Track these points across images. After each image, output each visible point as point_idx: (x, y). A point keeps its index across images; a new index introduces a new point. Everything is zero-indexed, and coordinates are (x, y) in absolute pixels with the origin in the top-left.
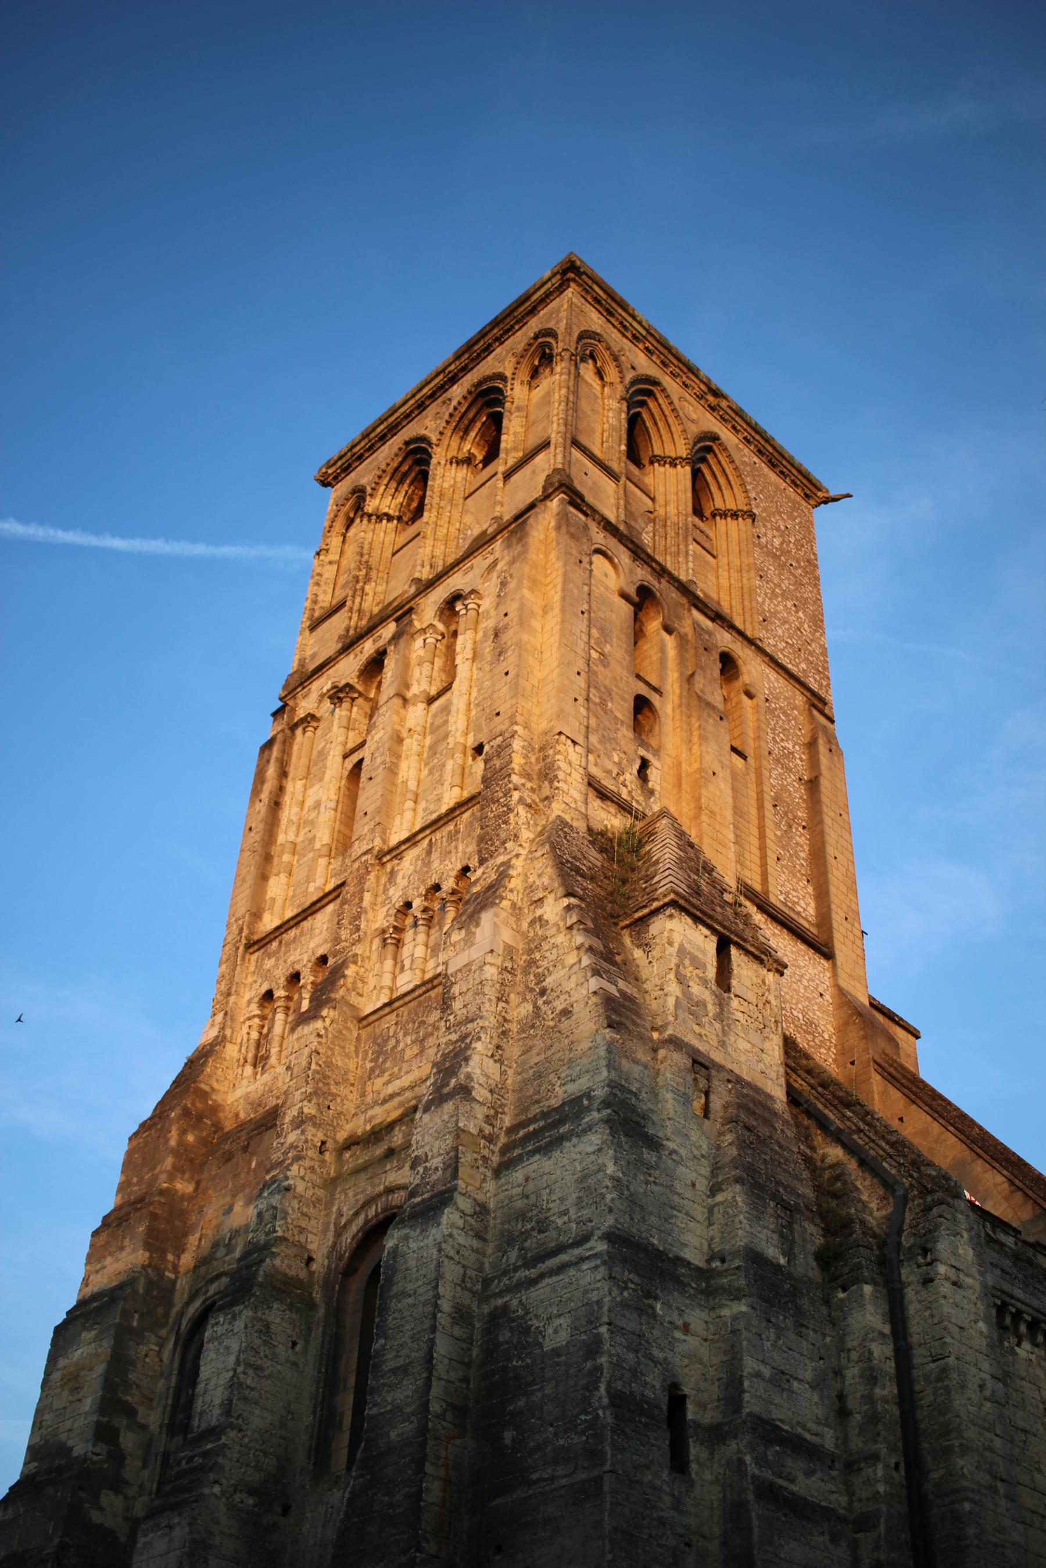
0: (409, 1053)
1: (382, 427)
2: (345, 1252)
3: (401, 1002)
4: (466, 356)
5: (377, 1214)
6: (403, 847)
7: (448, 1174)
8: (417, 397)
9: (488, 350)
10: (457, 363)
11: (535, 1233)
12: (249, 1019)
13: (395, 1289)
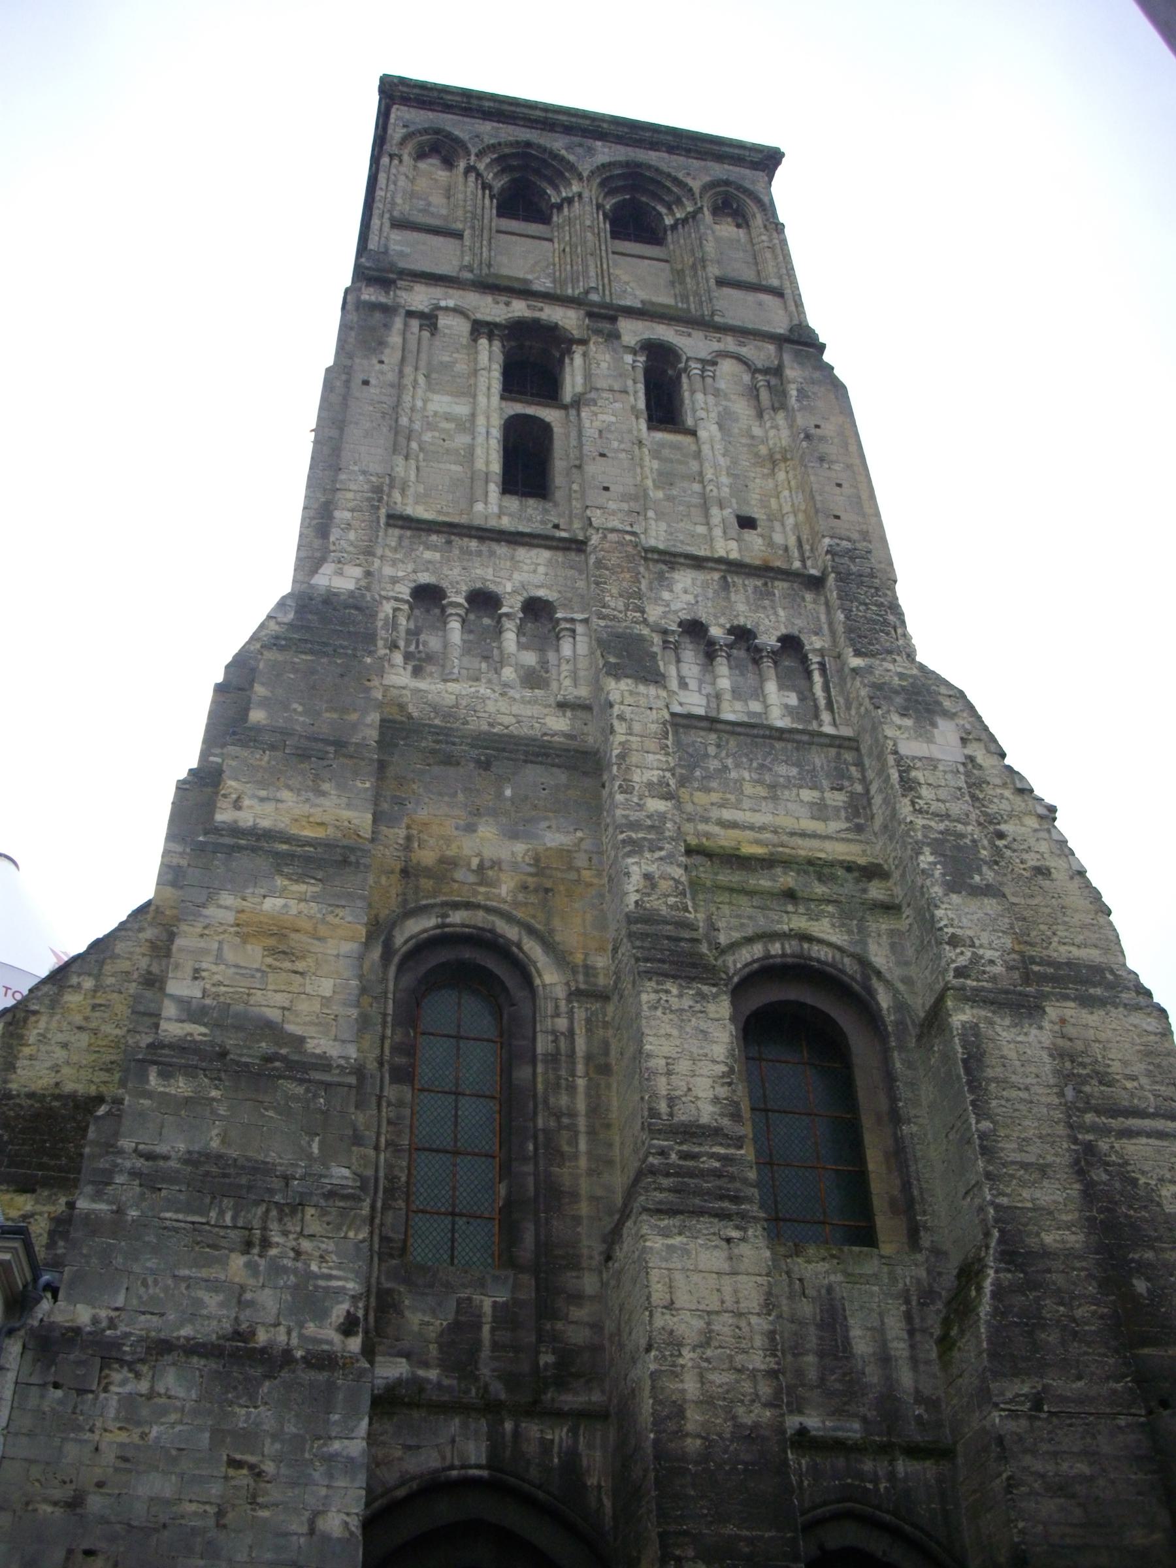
0: (748, 789)
1: (491, 104)
2: (734, 974)
3: (728, 728)
4: (626, 130)
5: (784, 955)
6: (682, 560)
7: (1016, 975)
8: (550, 115)
9: (688, 152)
10: (612, 127)
11: (1095, 1082)
12: (396, 599)
13: (990, 1073)
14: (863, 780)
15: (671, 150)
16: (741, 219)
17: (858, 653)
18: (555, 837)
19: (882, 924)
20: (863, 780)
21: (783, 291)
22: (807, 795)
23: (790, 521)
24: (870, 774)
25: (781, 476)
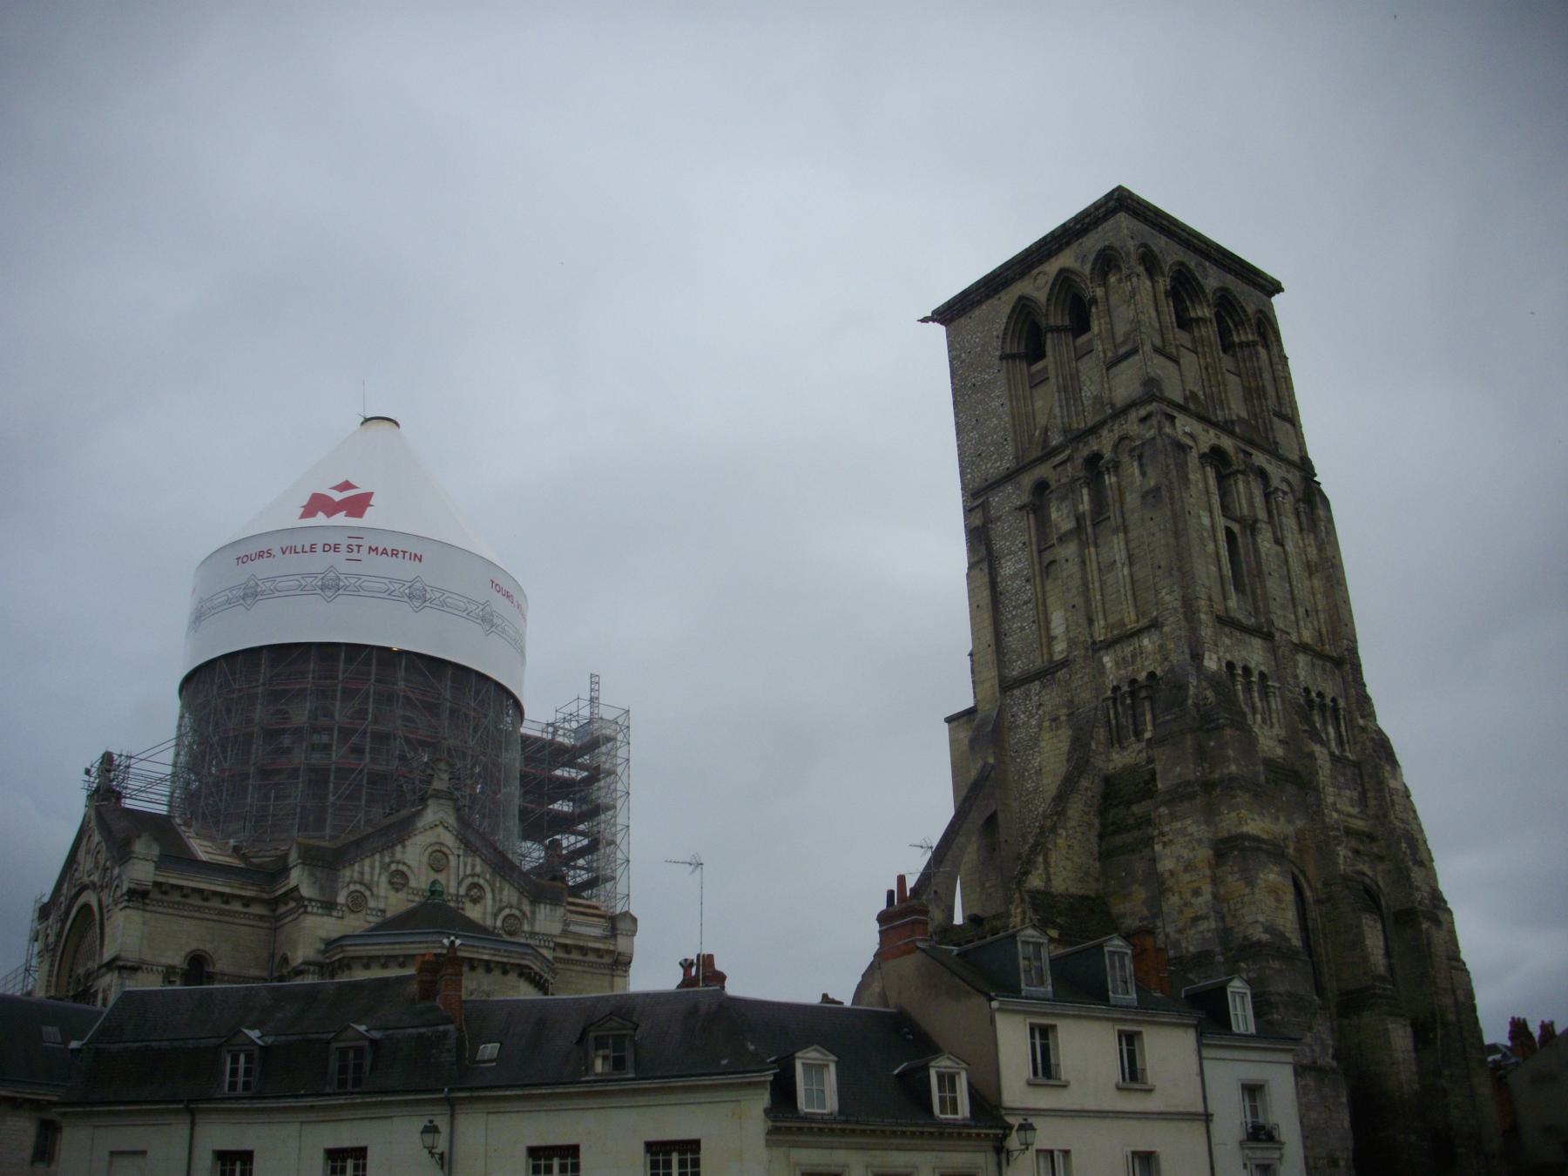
14: (1363, 785)
15: (1237, 275)
16: (1267, 347)
17: (1363, 717)
18: (1300, 824)
19: (1380, 867)
20: (1363, 785)
21: (1293, 420)
22: (1348, 793)
23: (1322, 616)
24: (1367, 786)
25: (1316, 582)
